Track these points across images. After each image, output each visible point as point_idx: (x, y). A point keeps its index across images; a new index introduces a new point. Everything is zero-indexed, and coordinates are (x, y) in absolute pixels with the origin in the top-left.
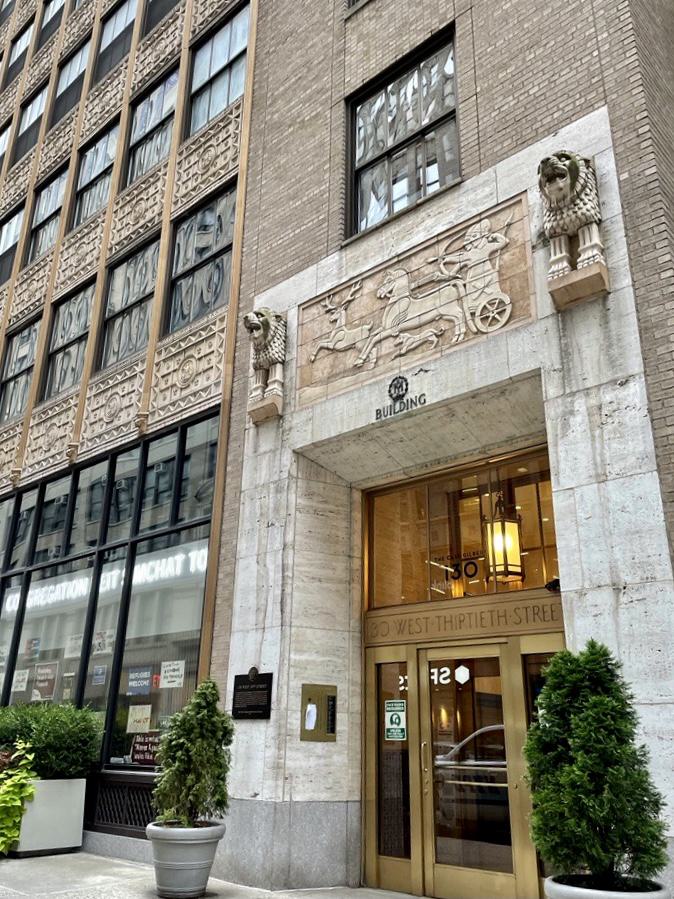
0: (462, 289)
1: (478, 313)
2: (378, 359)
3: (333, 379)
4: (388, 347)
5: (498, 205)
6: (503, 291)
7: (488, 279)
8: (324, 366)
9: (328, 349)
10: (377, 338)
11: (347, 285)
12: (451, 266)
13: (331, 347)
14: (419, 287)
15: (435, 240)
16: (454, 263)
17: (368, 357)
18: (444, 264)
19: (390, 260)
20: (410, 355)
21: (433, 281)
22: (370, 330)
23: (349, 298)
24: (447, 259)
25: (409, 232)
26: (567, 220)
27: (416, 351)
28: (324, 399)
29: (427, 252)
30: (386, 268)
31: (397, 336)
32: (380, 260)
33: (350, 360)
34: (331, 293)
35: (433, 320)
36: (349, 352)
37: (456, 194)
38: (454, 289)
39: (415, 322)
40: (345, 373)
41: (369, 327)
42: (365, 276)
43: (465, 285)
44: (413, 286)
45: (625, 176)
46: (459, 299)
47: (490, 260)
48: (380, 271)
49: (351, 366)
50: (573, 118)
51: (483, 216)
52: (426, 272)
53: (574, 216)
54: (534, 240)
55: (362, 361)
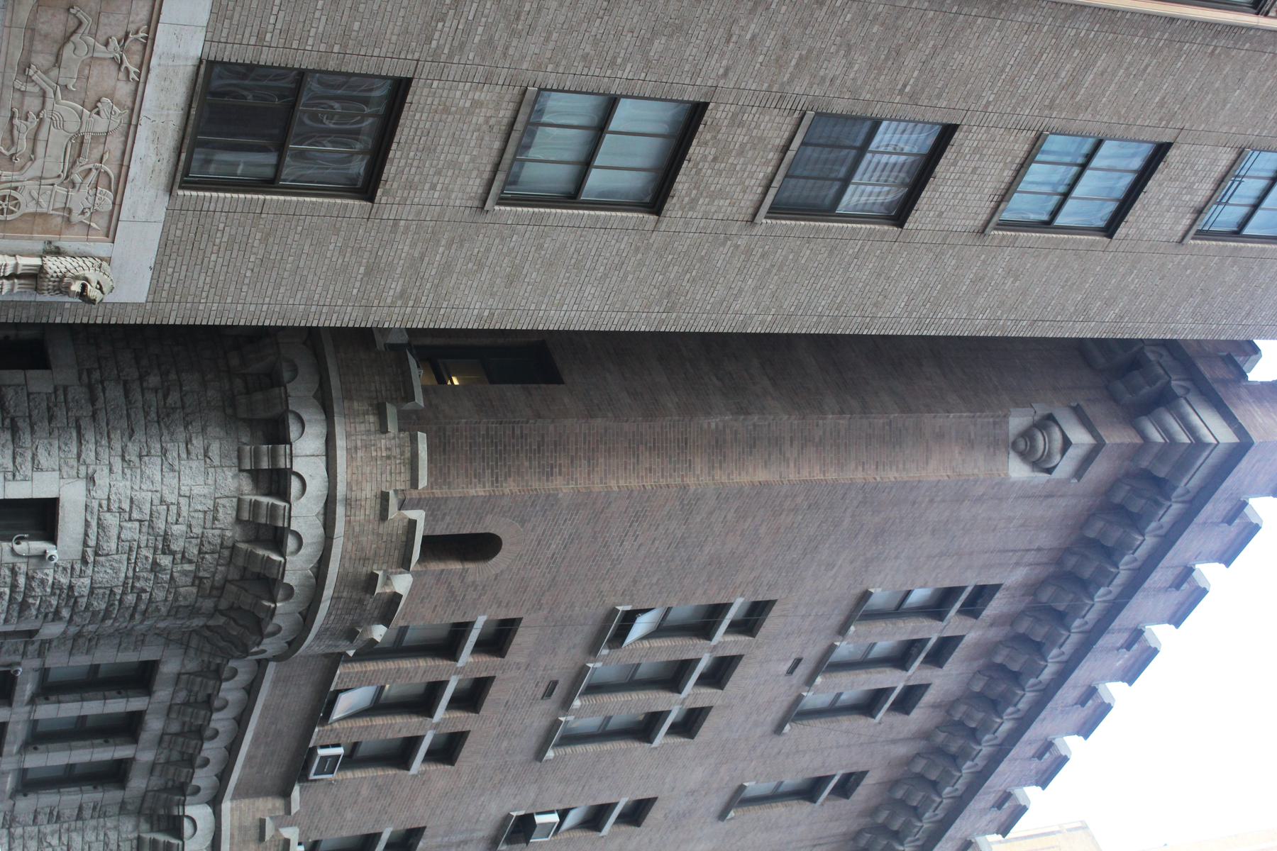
0: (50, 181)
1: (14, 193)
2: (23, 93)
3: (28, 35)
4: (32, 104)
5: (118, 220)
6: (24, 215)
7: (44, 204)
8: (53, 24)
9: (74, 32)
10: (50, 93)
11: (144, 65)
12: (84, 174)
13: (72, 39)
14: (82, 143)
15: (126, 163)
16: (85, 178)
17: (33, 81)
18: (90, 169)
19: (139, 116)
20: (7, 126)
21: (79, 156)
22: (66, 86)
23: (126, 63)
24: (94, 173)
25: (157, 139)
26: (45, 284)
27: (9, 133)
28: (7, 24)
29: (118, 154)
30: (132, 110)
31: (38, 116)
32: (146, 104)
33: (42, 59)
34: (148, 43)
35: (33, 152)
36: (52, 59)
37: (162, 187)
38: (55, 175)
39: (43, 135)
40: (29, 51)
41: (71, 87)
42: (141, 86)
43: (53, 185)
44: (88, 138)
45: (67, 306)
46: (41, 178)
47: (64, 208)
48: (134, 103)
49: (33, 60)
50: (155, 281)
51: (117, 207)
52: (95, 151)
53: (45, 288)
54: (57, 244)
55: (31, 72)
